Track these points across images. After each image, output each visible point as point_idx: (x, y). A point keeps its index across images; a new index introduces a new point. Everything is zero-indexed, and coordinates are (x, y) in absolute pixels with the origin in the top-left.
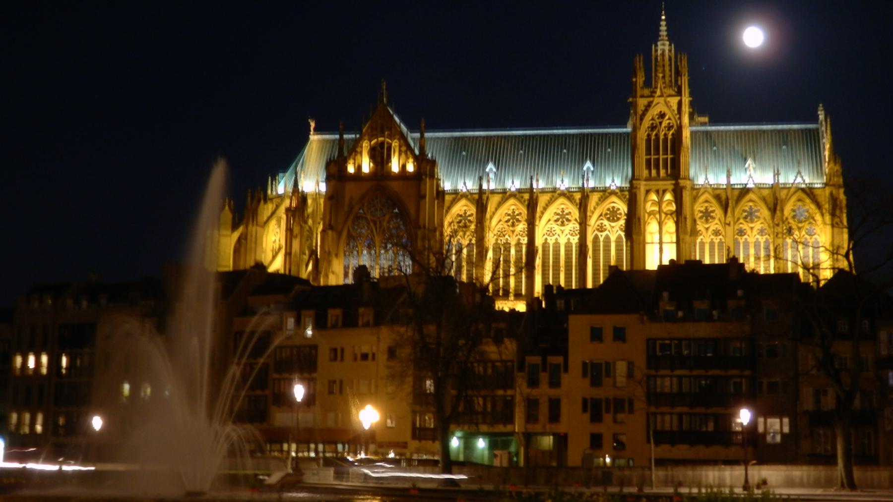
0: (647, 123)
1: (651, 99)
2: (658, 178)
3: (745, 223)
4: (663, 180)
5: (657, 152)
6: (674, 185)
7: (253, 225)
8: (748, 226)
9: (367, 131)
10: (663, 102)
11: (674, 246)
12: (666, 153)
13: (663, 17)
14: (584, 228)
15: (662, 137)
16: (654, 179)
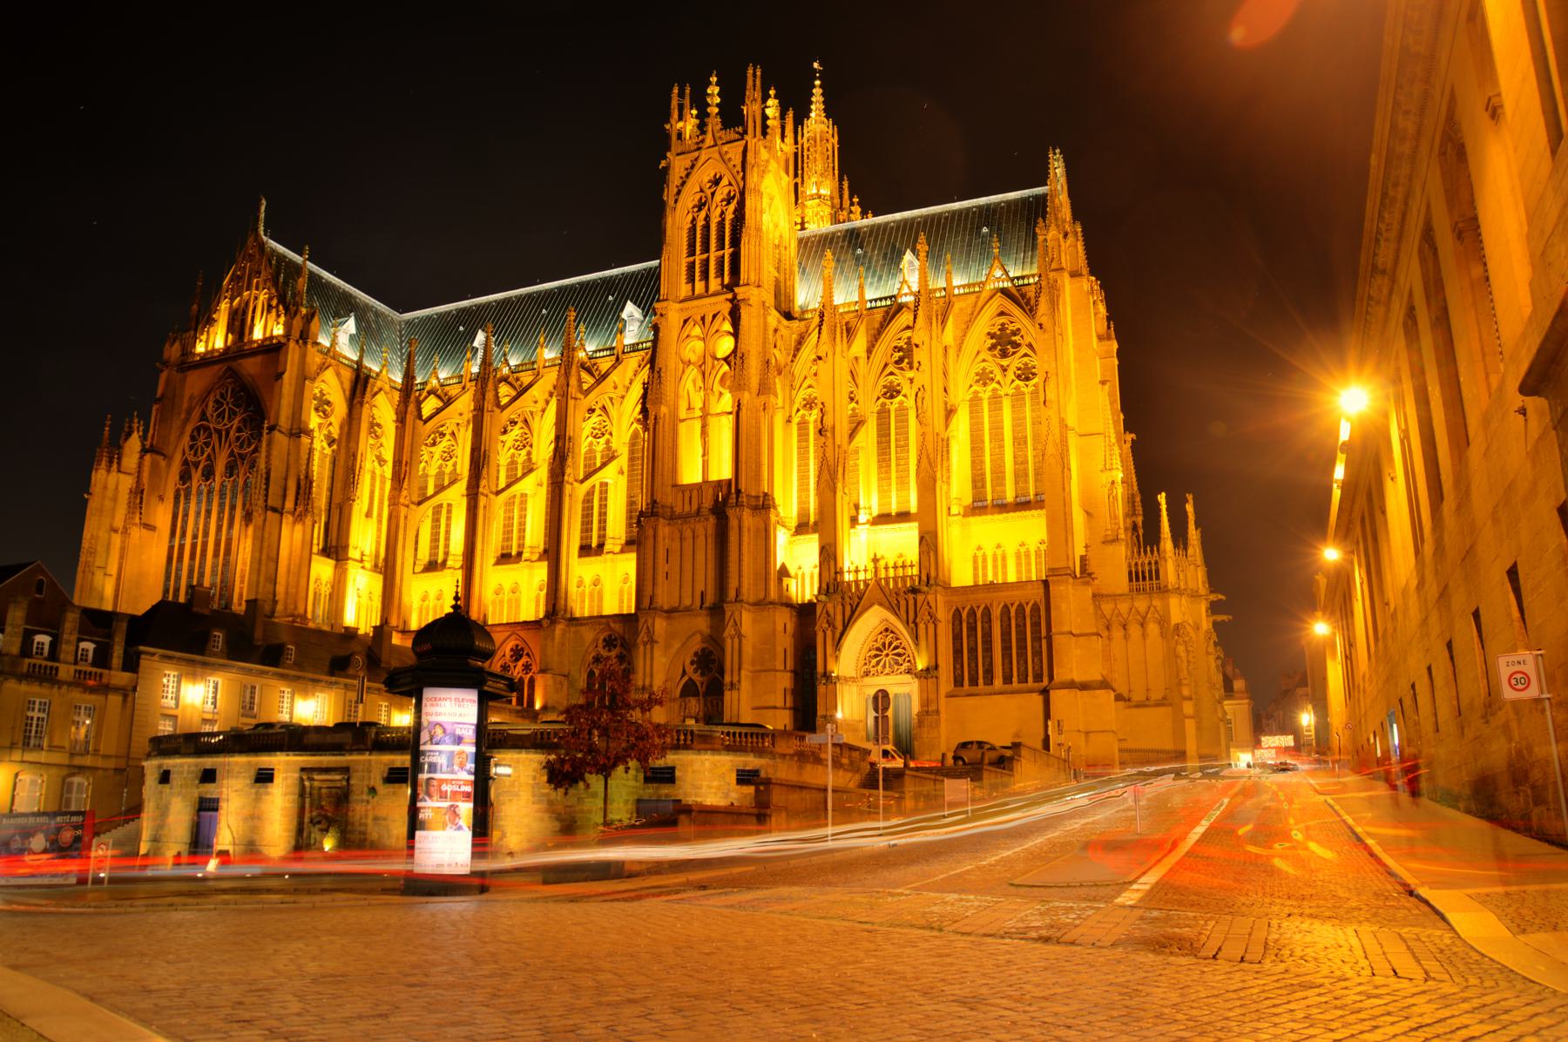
0: (689, 198)
1: (696, 154)
2: (707, 293)
3: (896, 371)
4: (716, 294)
5: (706, 249)
6: (731, 301)
7: (109, 471)
8: (904, 376)
9: (229, 283)
10: (716, 156)
11: (731, 418)
12: (721, 247)
13: (818, 83)
14: (564, 404)
15: (714, 220)
16: (700, 297)
